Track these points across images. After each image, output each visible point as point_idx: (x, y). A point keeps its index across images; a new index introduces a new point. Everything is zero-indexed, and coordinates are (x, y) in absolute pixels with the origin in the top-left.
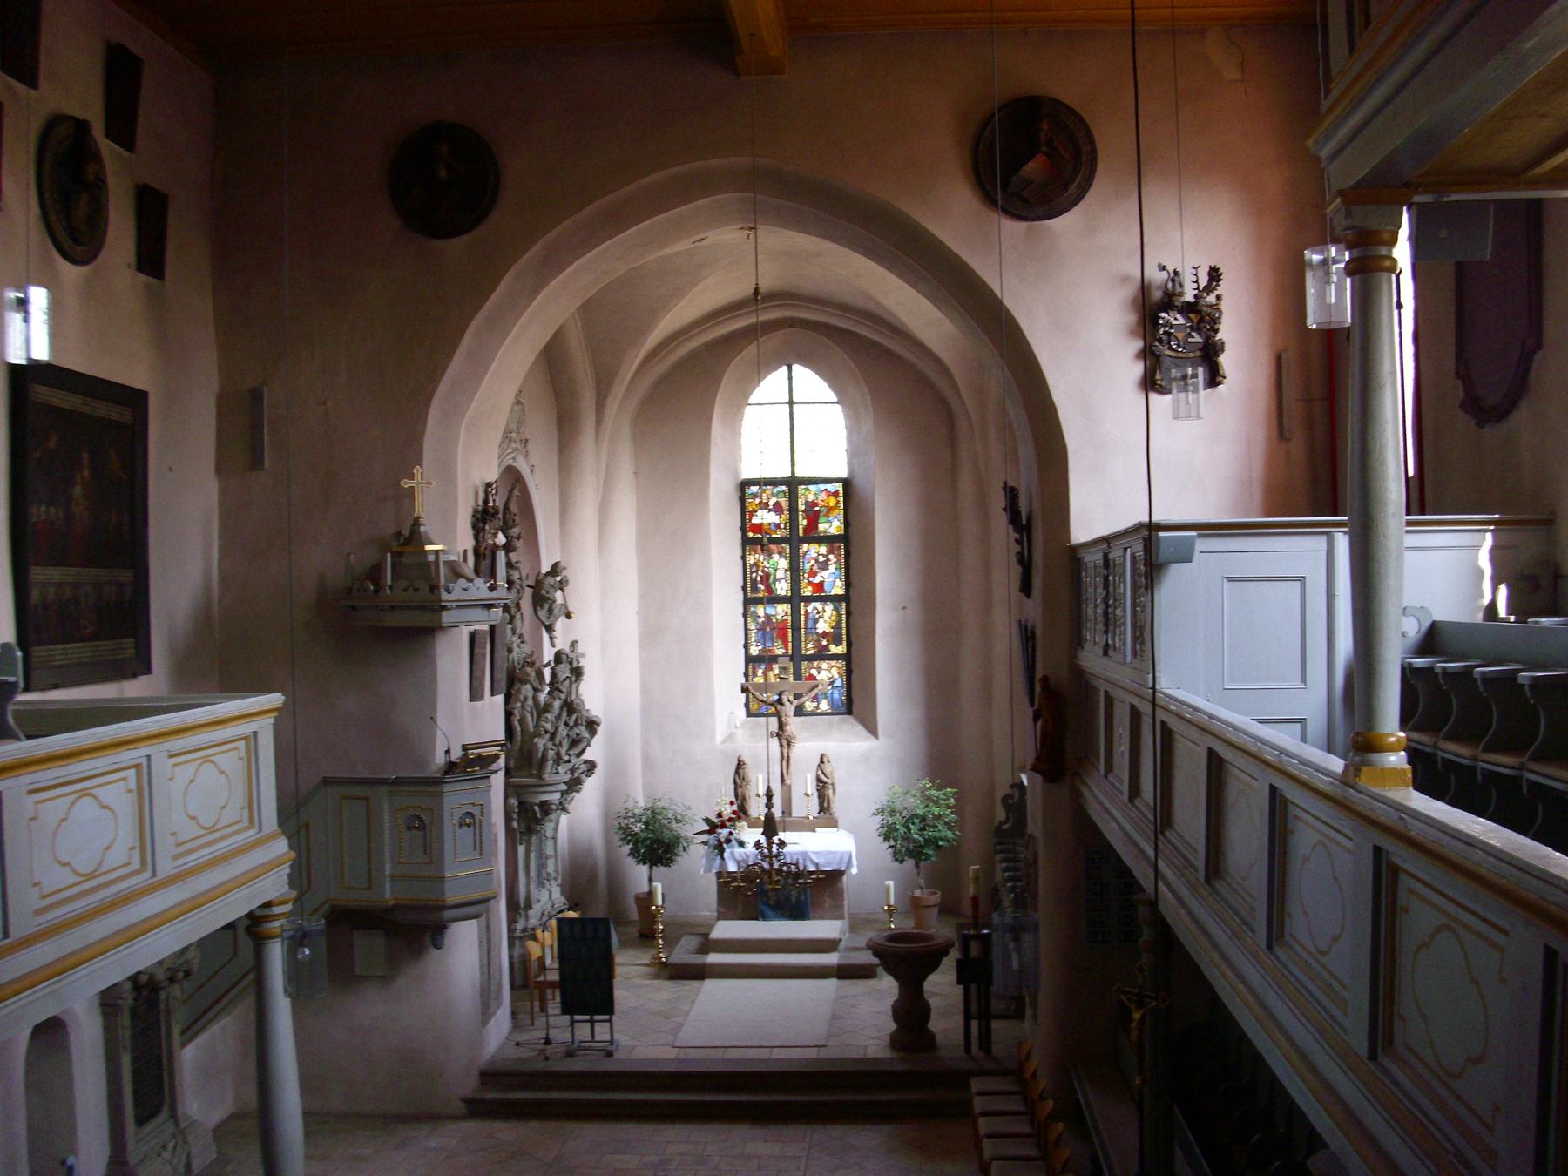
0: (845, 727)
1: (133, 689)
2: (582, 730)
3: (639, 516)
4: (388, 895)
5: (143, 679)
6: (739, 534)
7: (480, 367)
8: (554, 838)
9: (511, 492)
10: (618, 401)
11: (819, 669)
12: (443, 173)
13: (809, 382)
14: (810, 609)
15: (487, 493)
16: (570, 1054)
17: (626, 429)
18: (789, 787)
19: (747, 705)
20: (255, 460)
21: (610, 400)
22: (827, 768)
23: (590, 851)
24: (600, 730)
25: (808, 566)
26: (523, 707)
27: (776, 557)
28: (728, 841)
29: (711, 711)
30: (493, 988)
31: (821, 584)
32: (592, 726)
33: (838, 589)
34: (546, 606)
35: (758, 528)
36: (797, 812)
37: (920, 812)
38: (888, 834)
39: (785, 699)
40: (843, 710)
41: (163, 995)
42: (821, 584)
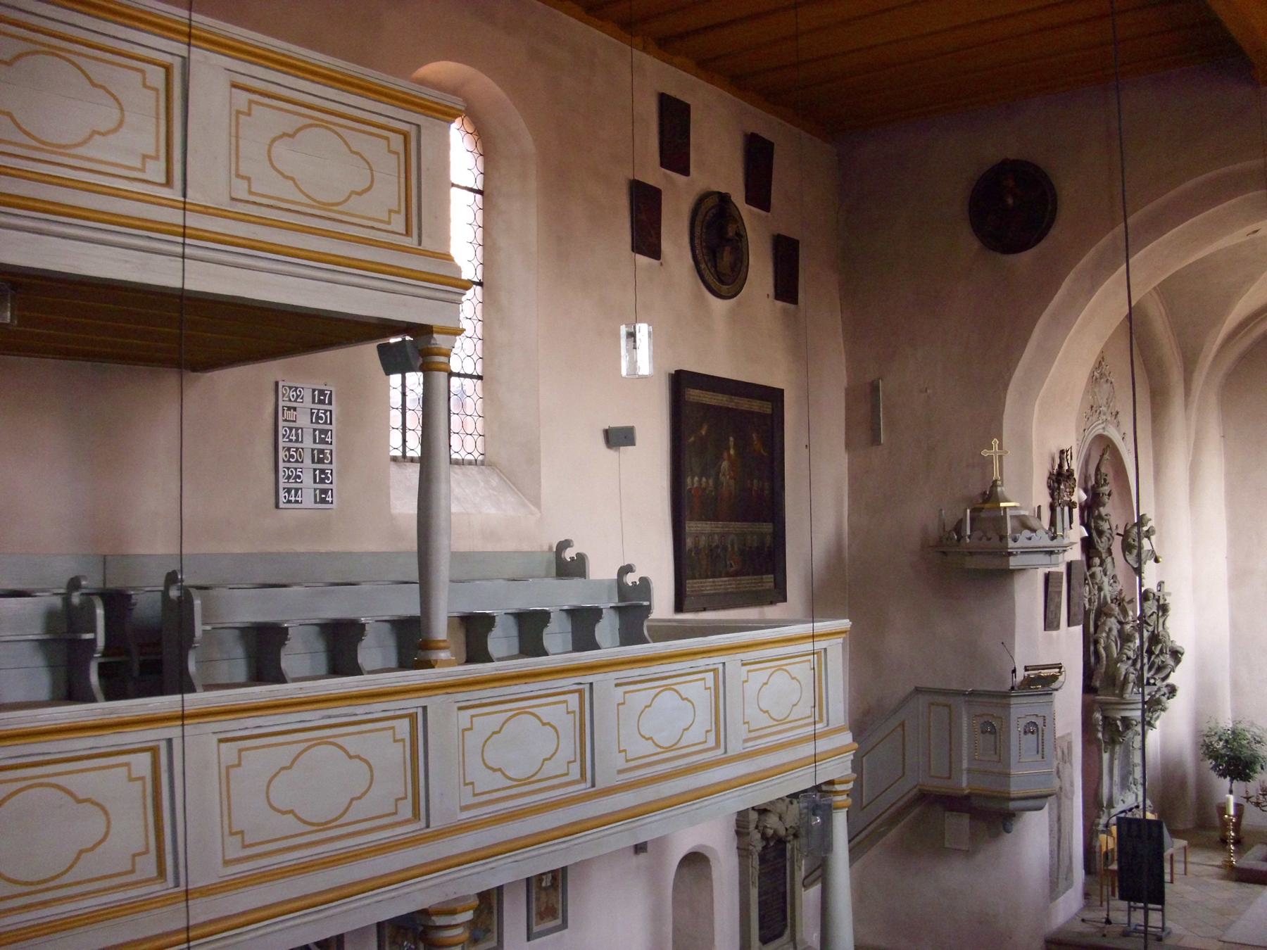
1: (771, 612)
3: (1228, 474)
4: (964, 785)
5: (781, 605)
7: (1048, 355)
9: (1102, 456)
10: (1204, 373)
12: (1010, 201)
15: (1061, 459)
16: (1126, 934)
17: (1213, 400)
20: (875, 440)
21: (1196, 374)
23: (1180, 764)
24: (1184, 658)
26: (1108, 637)
30: (1063, 869)
32: (1176, 655)
34: (1135, 552)
41: (789, 846)
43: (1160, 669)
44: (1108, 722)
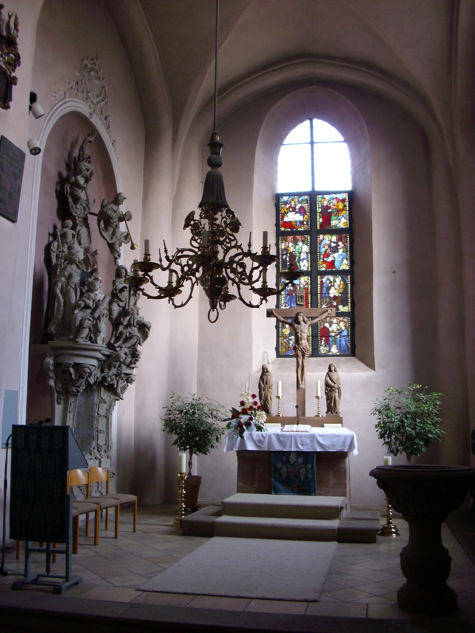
0: (350, 364)
2: (135, 331)
6: (275, 228)
8: (108, 417)
9: (86, 138)
11: (331, 324)
13: (325, 132)
14: (324, 280)
16: (16, 586)
18: (304, 390)
19: (277, 349)
22: (334, 376)
24: (152, 333)
25: (323, 250)
26: (68, 284)
27: (300, 244)
28: (248, 424)
29: (249, 348)
31: (333, 262)
33: (345, 266)
34: (111, 230)
35: (289, 225)
36: (310, 412)
37: (413, 409)
38: (385, 431)
39: (301, 319)
40: (349, 352)
42: (333, 262)
43: (127, 339)
44: (60, 368)
